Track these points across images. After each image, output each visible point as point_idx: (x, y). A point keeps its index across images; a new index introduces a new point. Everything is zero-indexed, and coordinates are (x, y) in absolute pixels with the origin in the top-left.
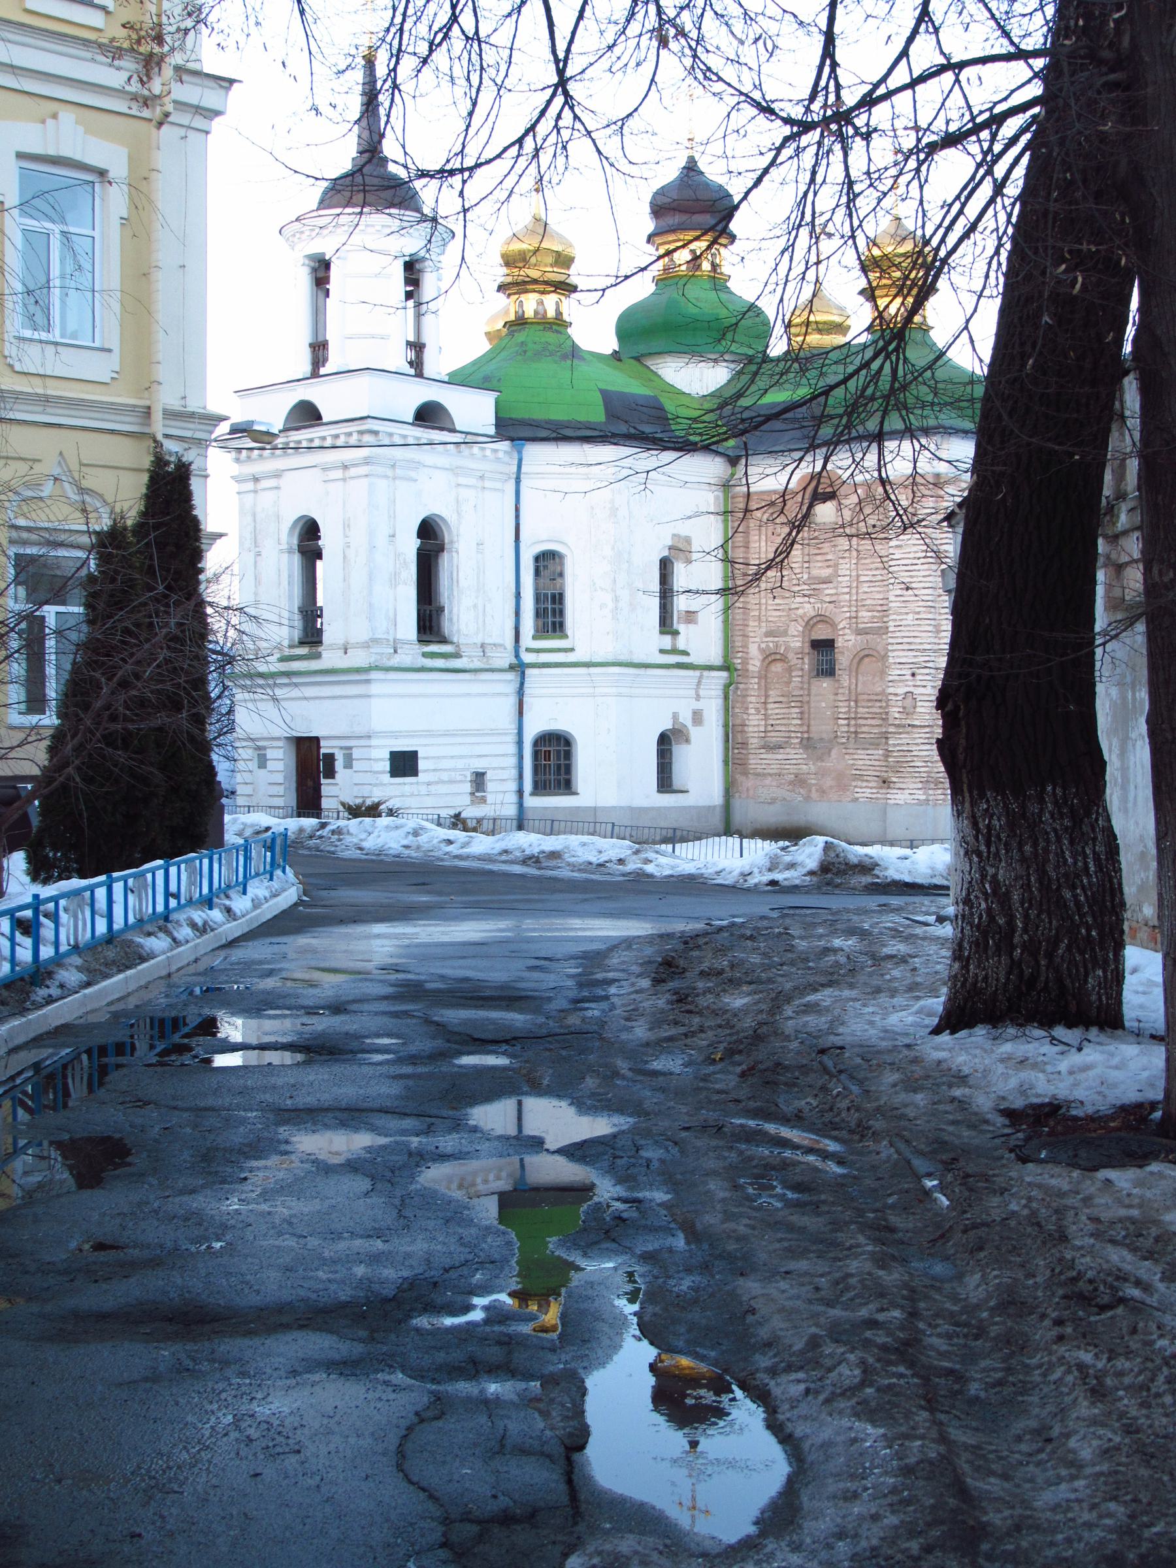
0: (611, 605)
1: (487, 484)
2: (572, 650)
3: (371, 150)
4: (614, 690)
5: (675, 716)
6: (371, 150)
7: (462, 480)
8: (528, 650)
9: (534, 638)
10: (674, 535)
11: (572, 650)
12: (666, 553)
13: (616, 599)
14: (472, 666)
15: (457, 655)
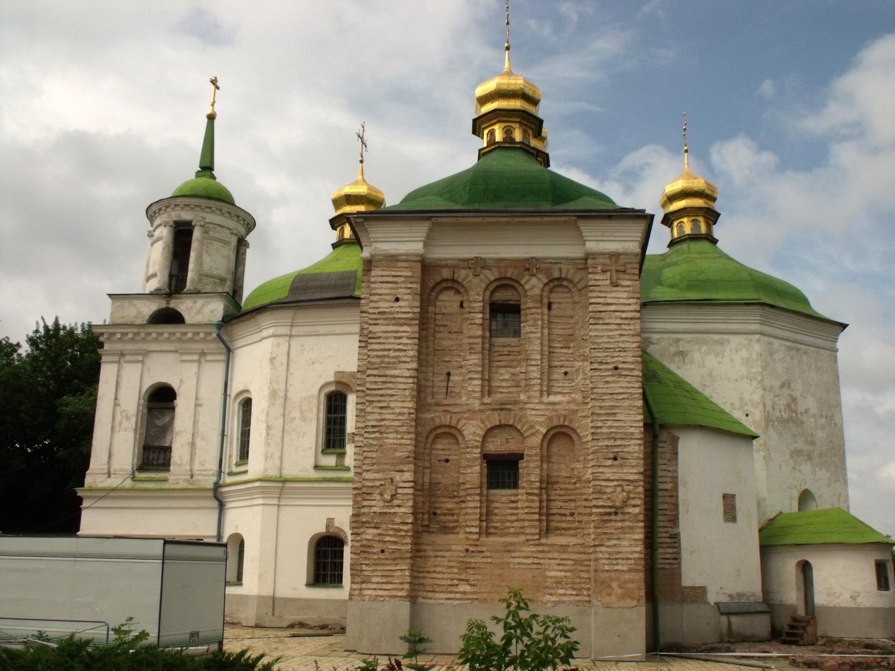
0: (264, 433)
1: (209, 358)
2: (246, 472)
3: (207, 168)
4: (260, 501)
5: (330, 522)
6: (207, 168)
7: (185, 358)
8: (231, 474)
9: (237, 465)
10: (337, 373)
11: (246, 472)
12: (332, 388)
13: (269, 428)
14: (176, 487)
15: (165, 480)
